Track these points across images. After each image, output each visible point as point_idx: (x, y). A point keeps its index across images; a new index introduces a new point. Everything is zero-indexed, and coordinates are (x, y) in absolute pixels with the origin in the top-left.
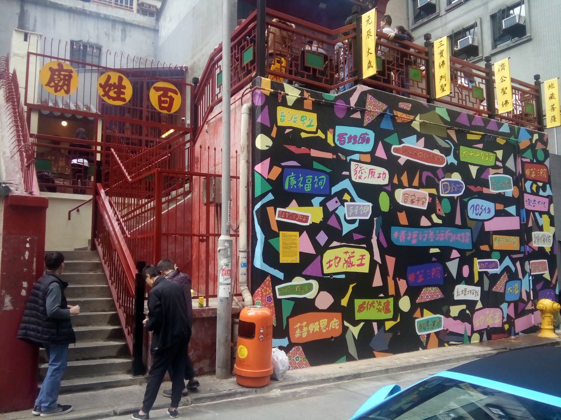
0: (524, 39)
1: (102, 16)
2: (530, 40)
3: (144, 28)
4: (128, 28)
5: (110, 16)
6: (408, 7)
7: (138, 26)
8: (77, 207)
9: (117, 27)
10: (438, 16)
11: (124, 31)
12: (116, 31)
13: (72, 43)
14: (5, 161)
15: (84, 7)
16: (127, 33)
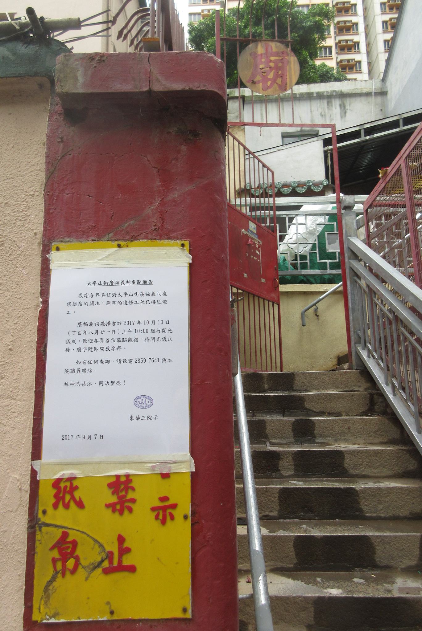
1: (315, 95)
3: (368, 94)
4: (347, 101)
7: (360, 95)
8: (315, 304)
9: (333, 104)
11: (343, 107)
12: (334, 109)
16: (347, 107)
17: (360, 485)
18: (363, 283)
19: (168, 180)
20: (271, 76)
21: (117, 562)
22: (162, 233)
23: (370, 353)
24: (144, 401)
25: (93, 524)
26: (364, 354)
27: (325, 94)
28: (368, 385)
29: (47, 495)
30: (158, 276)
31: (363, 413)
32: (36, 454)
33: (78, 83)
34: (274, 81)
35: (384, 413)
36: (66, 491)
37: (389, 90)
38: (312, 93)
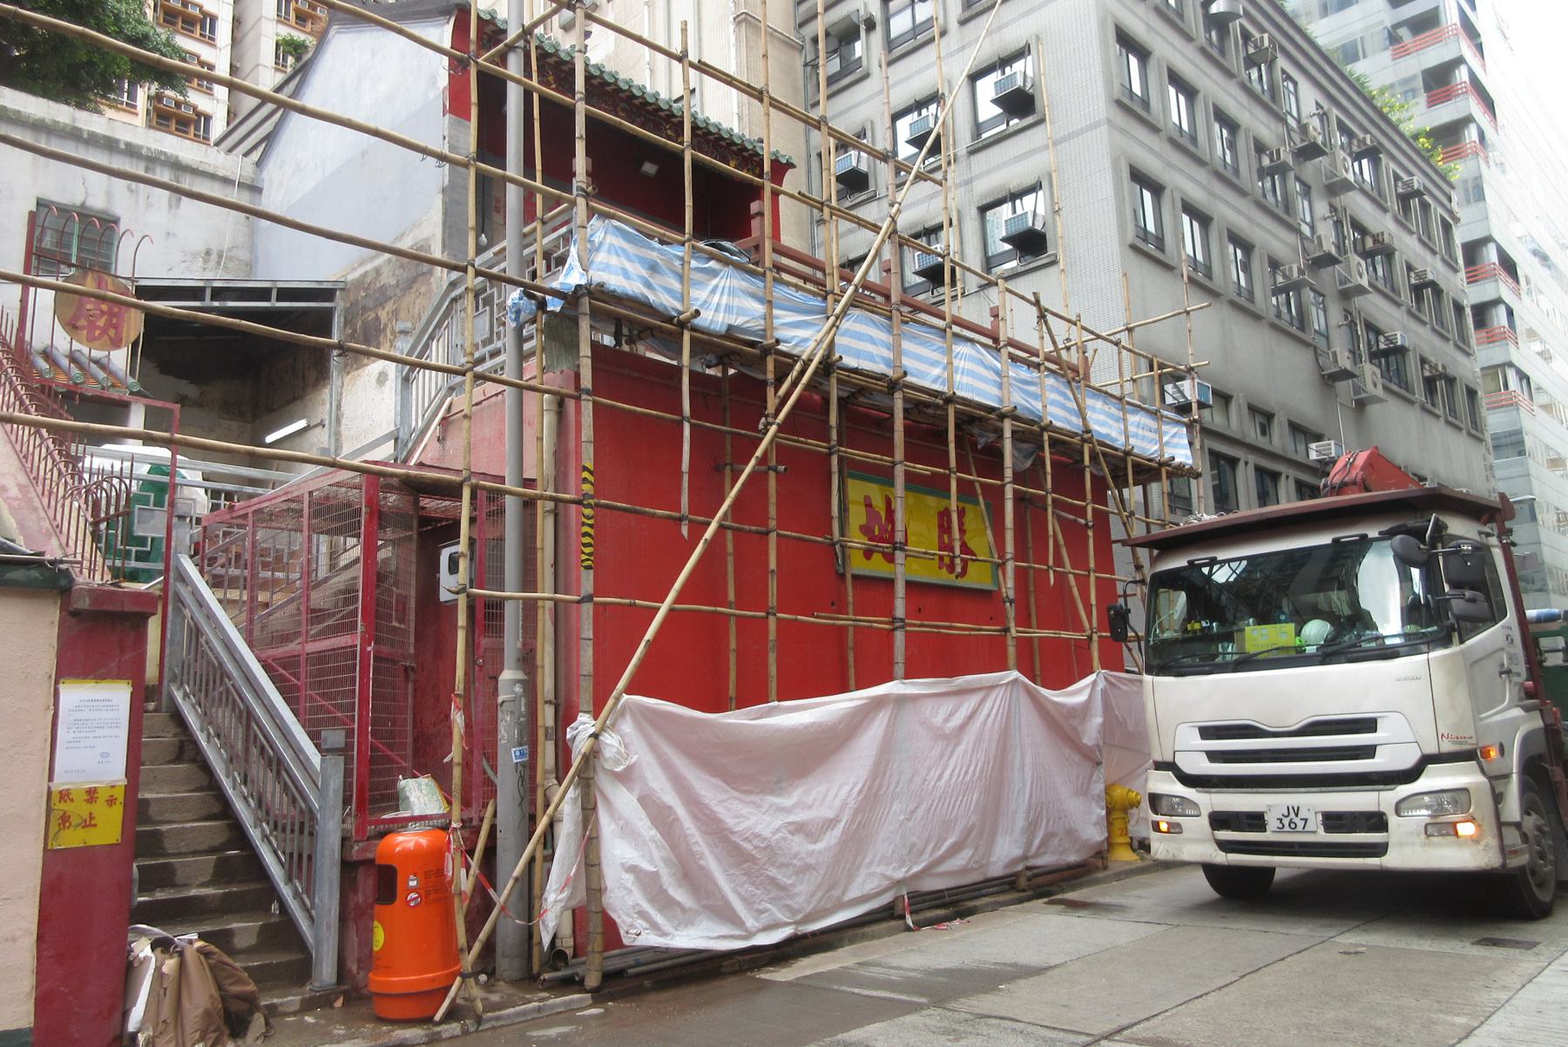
0: (1043, 260)
1: (122, 146)
2: (1054, 263)
5: (141, 147)
6: (809, 172)
10: (872, 198)
13: (41, 203)
14: (11, 508)
15: (74, 120)
17: (164, 828)
18: (187, 613)
19: (123, 651)
20: (101, 322)
21: (89, 823)
22: (118, 676)
23: (186, 695)
24: (105, 755)
25: (78, 809)
26: (179, 696)
27: (144, 152)
28: (178, 730)
29: (56, 797)
30: (118, 695)
31: (169, 762)
32: (51, 779)
33: (84, 604)
34: (104, 331)
35: (193, 761)
36: (65, 795)
37: (265, 186)
38: (117, 141)
